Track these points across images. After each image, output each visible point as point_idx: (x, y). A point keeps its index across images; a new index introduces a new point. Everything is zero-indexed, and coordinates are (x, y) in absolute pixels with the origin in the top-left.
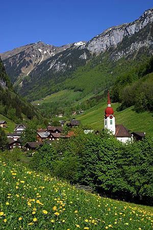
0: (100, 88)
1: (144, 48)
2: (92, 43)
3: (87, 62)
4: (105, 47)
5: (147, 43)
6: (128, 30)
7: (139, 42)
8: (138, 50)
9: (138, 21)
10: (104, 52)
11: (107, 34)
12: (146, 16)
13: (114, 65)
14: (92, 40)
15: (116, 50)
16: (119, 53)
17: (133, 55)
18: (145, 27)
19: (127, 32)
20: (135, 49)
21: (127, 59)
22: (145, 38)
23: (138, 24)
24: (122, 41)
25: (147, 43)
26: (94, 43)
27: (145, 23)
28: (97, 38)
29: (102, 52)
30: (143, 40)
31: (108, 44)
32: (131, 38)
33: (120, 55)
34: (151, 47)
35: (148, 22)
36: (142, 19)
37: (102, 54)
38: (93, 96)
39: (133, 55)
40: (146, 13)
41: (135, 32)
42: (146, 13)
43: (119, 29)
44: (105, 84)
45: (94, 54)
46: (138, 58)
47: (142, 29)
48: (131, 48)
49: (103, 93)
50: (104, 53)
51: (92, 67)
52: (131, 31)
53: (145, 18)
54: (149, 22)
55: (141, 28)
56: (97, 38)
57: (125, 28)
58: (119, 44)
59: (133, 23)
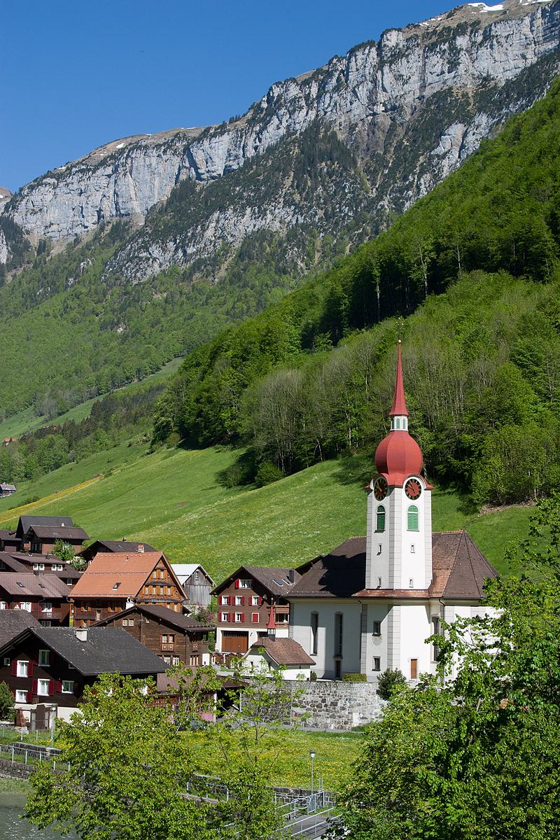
0: (68, 393)
1: (262, 236)
2: (36, 196)
3: (9, 278)
4: (91, 220)
5: (278, 219)
6: (199, 156)
7: (243, 208)
8: (237, 245)
9: (241, 124)
10: (86, 239)
11: (103, 163)
12: (275, 105)
13: (132, 297)
14: (38, 183)
15: (141, 233)
16: (155, 251)
17: (215, 262)
18: (270, 150)
19: (193, 164)
20: (223, 237)
21: (187, 276)
22: (270, 195)
23: (241, 134)
24: (170, 202)
25: (278, 219)
26: (43, 196)
27: (273, 134)
28: (59, 177)
29: (77, 241)
30: (259, 204)
31: (109, 208)
32: (210, 190)
33: (160, 258)
34: (292, 235)
35: (282, 131)
36: (261, 117)
37: (78, 251)
38: (36, 423)
39: (215, 262)
40: (277, 91)
41: (227, 170)
42: (277, 91)
43: (158, 146)
44: (92, 377)
45: (43, 247)
46: (235, 277)
47: (257, 159)
48: (209, 233)
49: (80, 414)
50: (88, 246)
51: (31, 300)
52: (208, 160)
53: (271, 112)
54: (289, 133)
55: (251, 153)
56: (59, 177)
57: (187, 150)
58: (153, 214)
59: (222, 130)
